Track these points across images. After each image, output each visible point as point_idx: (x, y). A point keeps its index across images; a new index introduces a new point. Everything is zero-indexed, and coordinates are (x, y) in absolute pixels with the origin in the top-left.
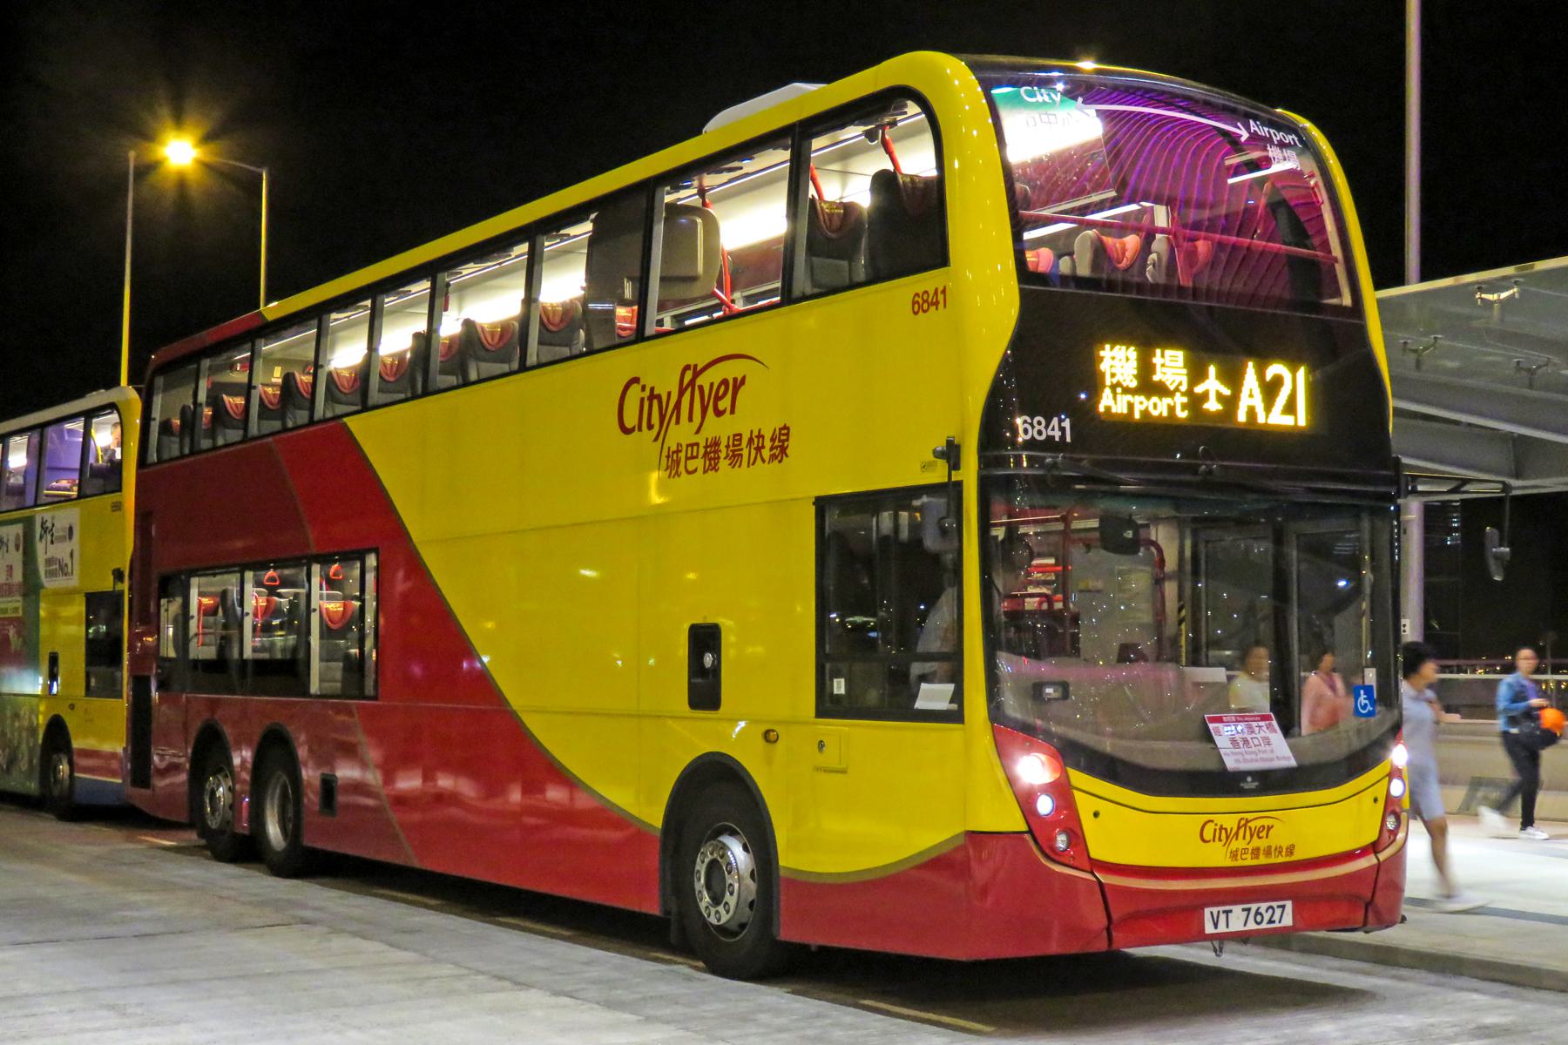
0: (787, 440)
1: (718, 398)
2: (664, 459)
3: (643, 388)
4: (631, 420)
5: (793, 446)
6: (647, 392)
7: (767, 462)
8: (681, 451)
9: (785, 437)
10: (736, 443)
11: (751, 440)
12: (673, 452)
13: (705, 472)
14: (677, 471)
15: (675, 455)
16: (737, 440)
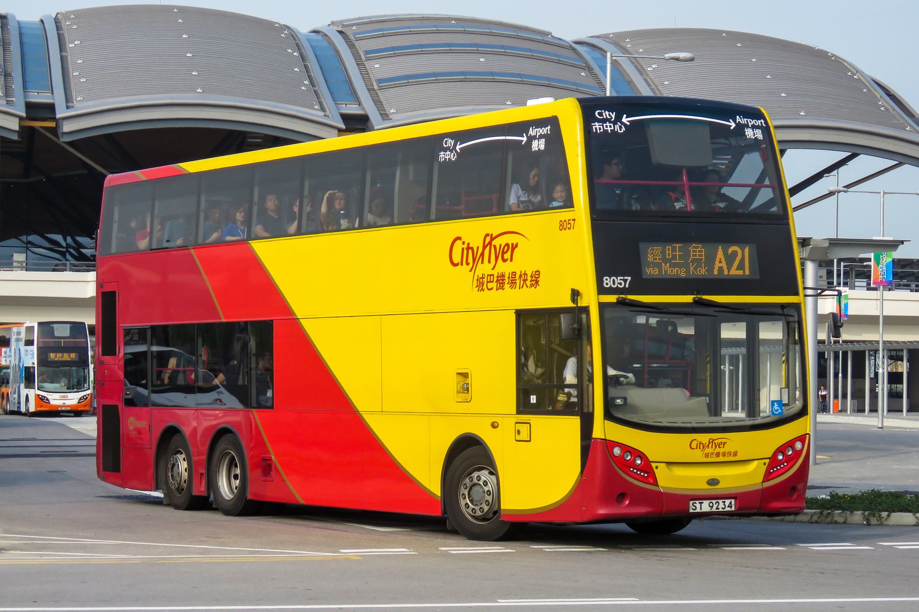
0: (539, 277)
1: (503, 253)
2: (475, 282)
3: (464, 243)
4: (456, 259)
5: (541, 280)
6: (465, 246)
7: (529, 285)
8: (484, 278)
10: (513, 276)
11: (520, 276)
12: (480, 278)
13: (497, 290)
15: (481, 281)
16: (514, 275)
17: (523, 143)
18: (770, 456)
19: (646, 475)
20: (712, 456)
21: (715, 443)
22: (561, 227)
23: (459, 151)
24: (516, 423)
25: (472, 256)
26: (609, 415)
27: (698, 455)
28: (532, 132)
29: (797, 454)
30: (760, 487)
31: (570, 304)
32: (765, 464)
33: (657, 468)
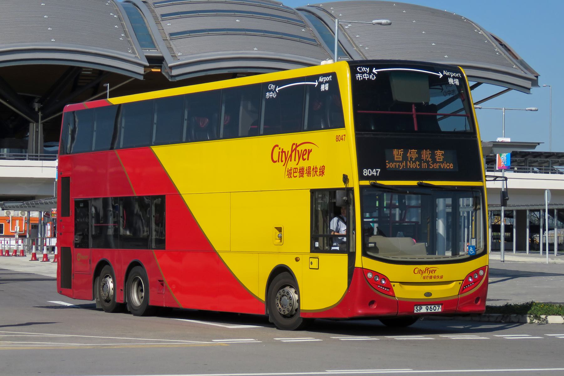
0: (324, 170)
1: (303, 155)
2: (286, 172)
3: (280, 149)
4: (275, 158)
5: (325, 171)
6: (281, 150)
7: (318, 175)
8: (292, 170)
9: (324, 169)
11: (313, 169)
12: (289, 170)
13: (299, 177)
14: (290, 176)
15: (290, 171)
17: (316, 86)
18: (463, 279)
19: (388, 290)
20: (427, 278)
21: (429, 270)
22: (337, 139)
23: (278, 92)
24: (310, 258)
25: (284, 157)
26: (364, 254)
27: (418, 278)
28: (321, 80)
29: (481, 277)
30: (456, 297)
31: (343, 186)
32: (460, 283)
33: (394, 286)
